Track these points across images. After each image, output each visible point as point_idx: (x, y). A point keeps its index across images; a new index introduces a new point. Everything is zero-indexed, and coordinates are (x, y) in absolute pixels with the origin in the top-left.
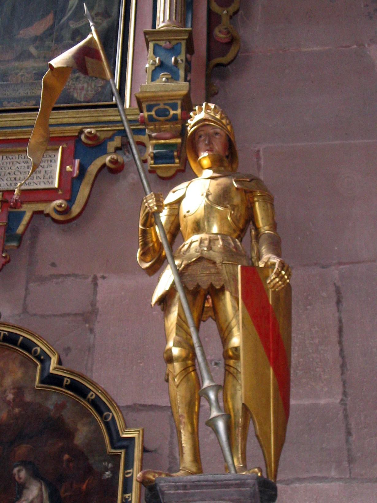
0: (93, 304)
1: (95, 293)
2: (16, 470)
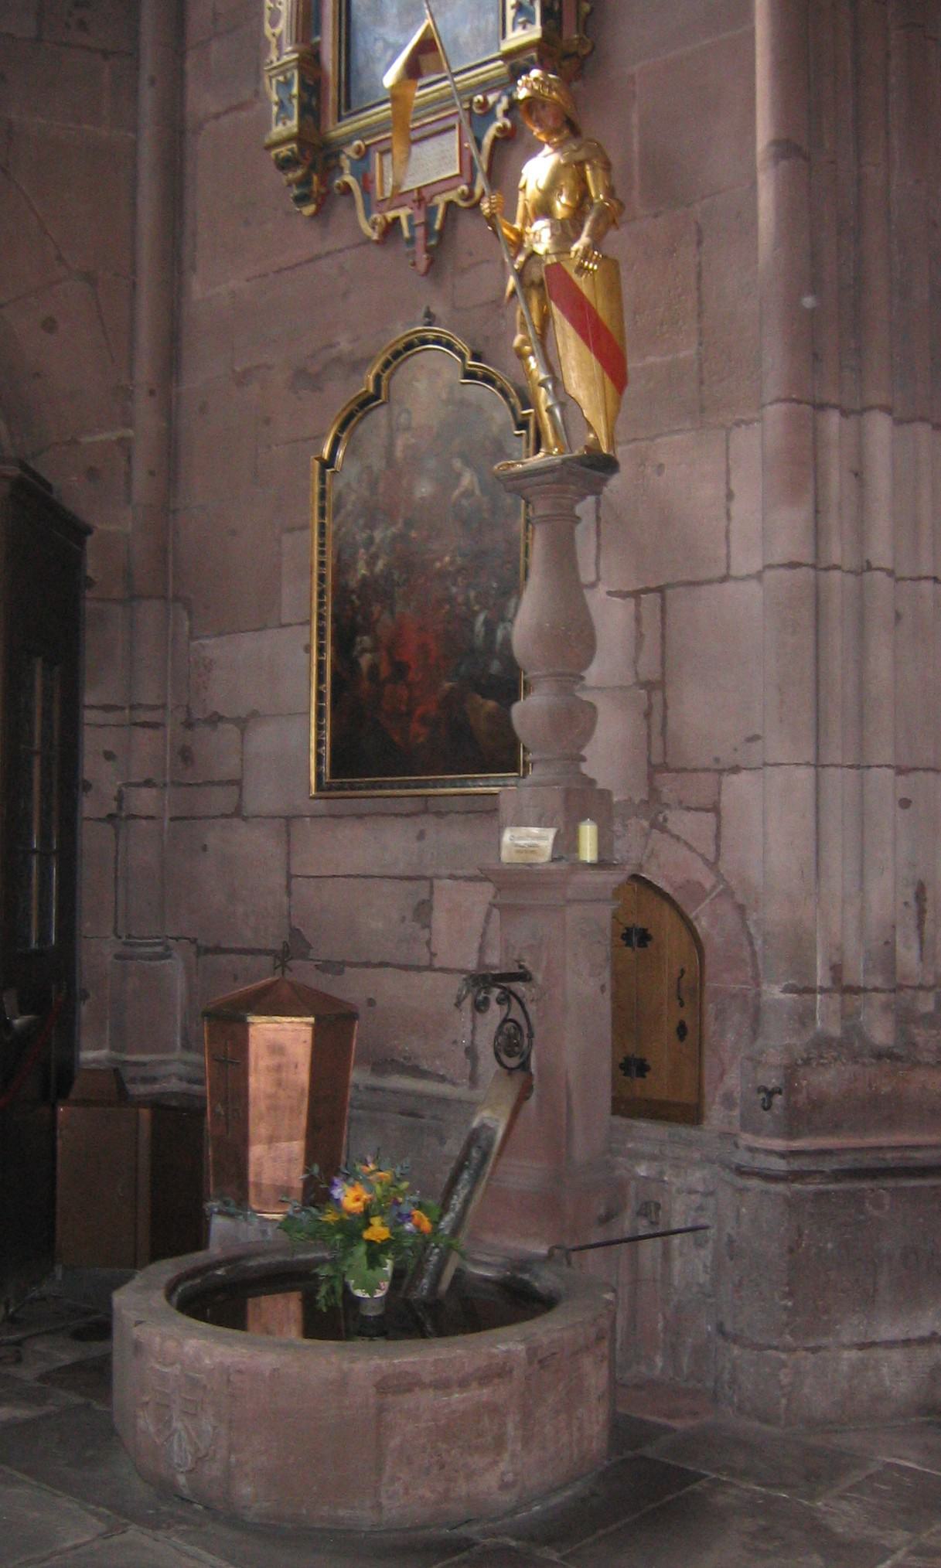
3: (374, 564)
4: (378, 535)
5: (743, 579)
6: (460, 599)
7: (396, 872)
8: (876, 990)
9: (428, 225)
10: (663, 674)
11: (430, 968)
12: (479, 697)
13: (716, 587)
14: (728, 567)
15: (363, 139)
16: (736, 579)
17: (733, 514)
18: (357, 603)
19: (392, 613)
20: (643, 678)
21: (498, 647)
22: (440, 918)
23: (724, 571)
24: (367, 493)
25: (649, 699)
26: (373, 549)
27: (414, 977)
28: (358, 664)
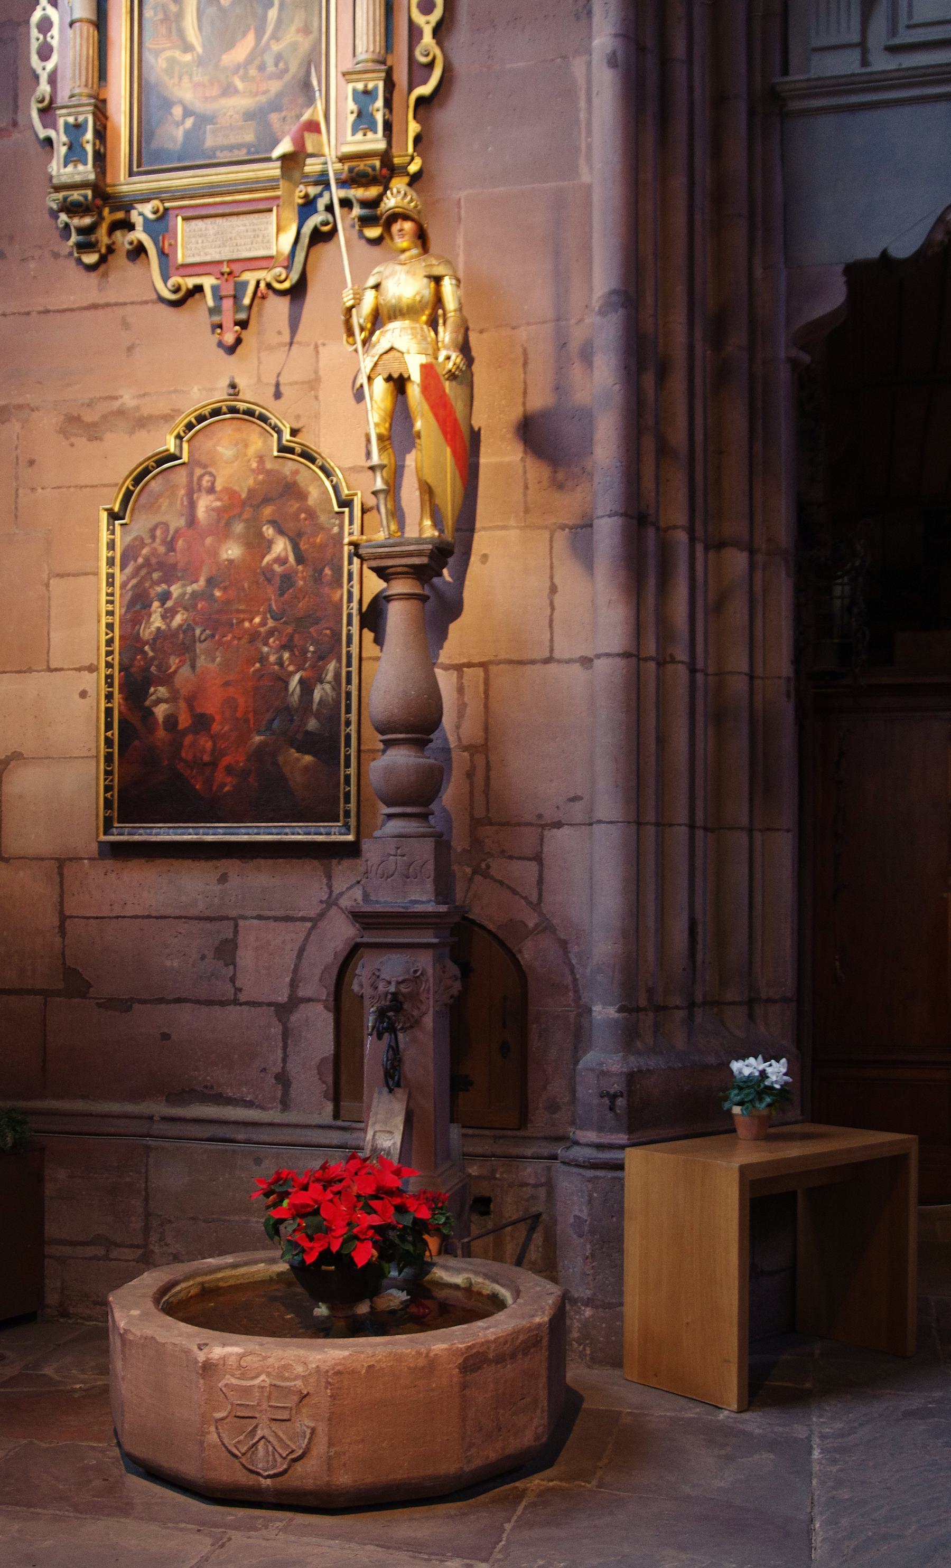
0: (316, 372)
1: (317, 361)
2: (265, 528)
3: (173, 617)
4: (176, 590)
5: (568, 661)
6: (272, 659)
7: (193, 912)
8: (677, 1007)
9: (237, 298)
10: (487, 739)
11: (236, 1002)
12: (293, 750)
13: (538, 667)
14: (552, 650)
15: (162, 201)
16: (559, 661)
17: (556, 605)
18: (151, 654)
19: (193, 667)
20: (465, 742)
21: (315, 707)
22: (246, 957)
23: (547, 654)
24: (162, 549)
25: (472, 761)
26: (169, 604)
27: (217, 1011)
28: (153, 713)
